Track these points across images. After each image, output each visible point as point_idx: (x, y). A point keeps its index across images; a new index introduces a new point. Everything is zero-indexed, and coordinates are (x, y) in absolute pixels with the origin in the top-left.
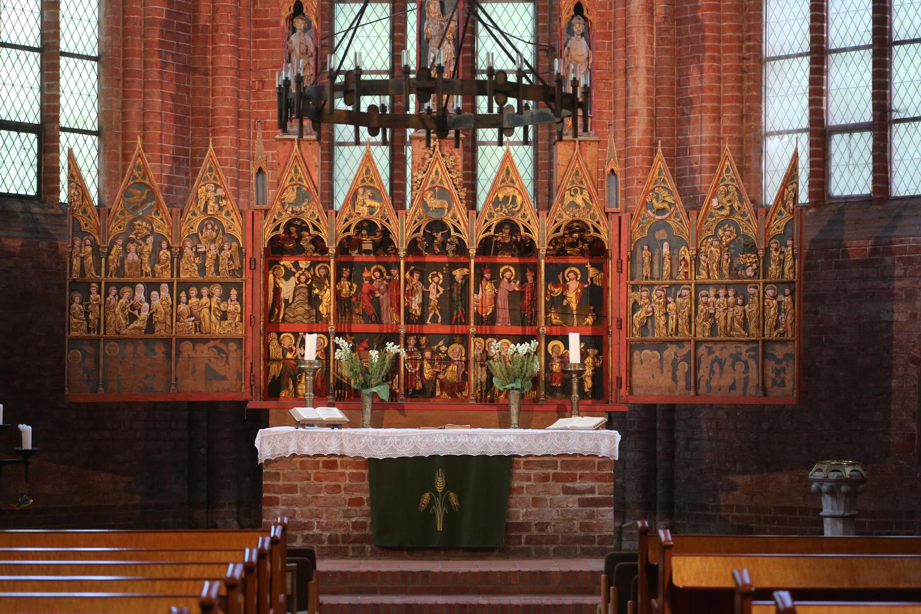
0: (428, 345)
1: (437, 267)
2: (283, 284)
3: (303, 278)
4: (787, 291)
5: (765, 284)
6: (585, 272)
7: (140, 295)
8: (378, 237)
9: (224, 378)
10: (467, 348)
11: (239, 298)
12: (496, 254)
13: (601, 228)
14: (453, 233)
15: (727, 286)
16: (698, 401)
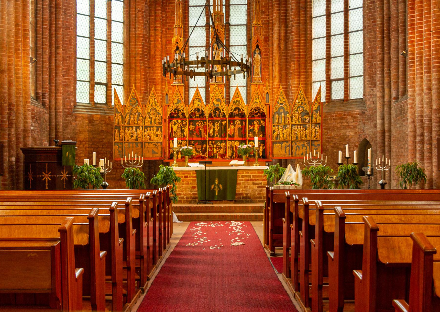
0: (215, 143)
1: (218, 121)
2: (173, 127)
3: (179, 125)
4: (318, 126)
5: (312, 124)
6: (260, 122)
7: (134, 130)
8: (201, 113)
9: (157, 153)
10: (226, 144)
11: (161, 131)
12: (234, 117)
13: (264, 109)
14: (222, 111)
15: (301, 125)
16: (292, 158)
